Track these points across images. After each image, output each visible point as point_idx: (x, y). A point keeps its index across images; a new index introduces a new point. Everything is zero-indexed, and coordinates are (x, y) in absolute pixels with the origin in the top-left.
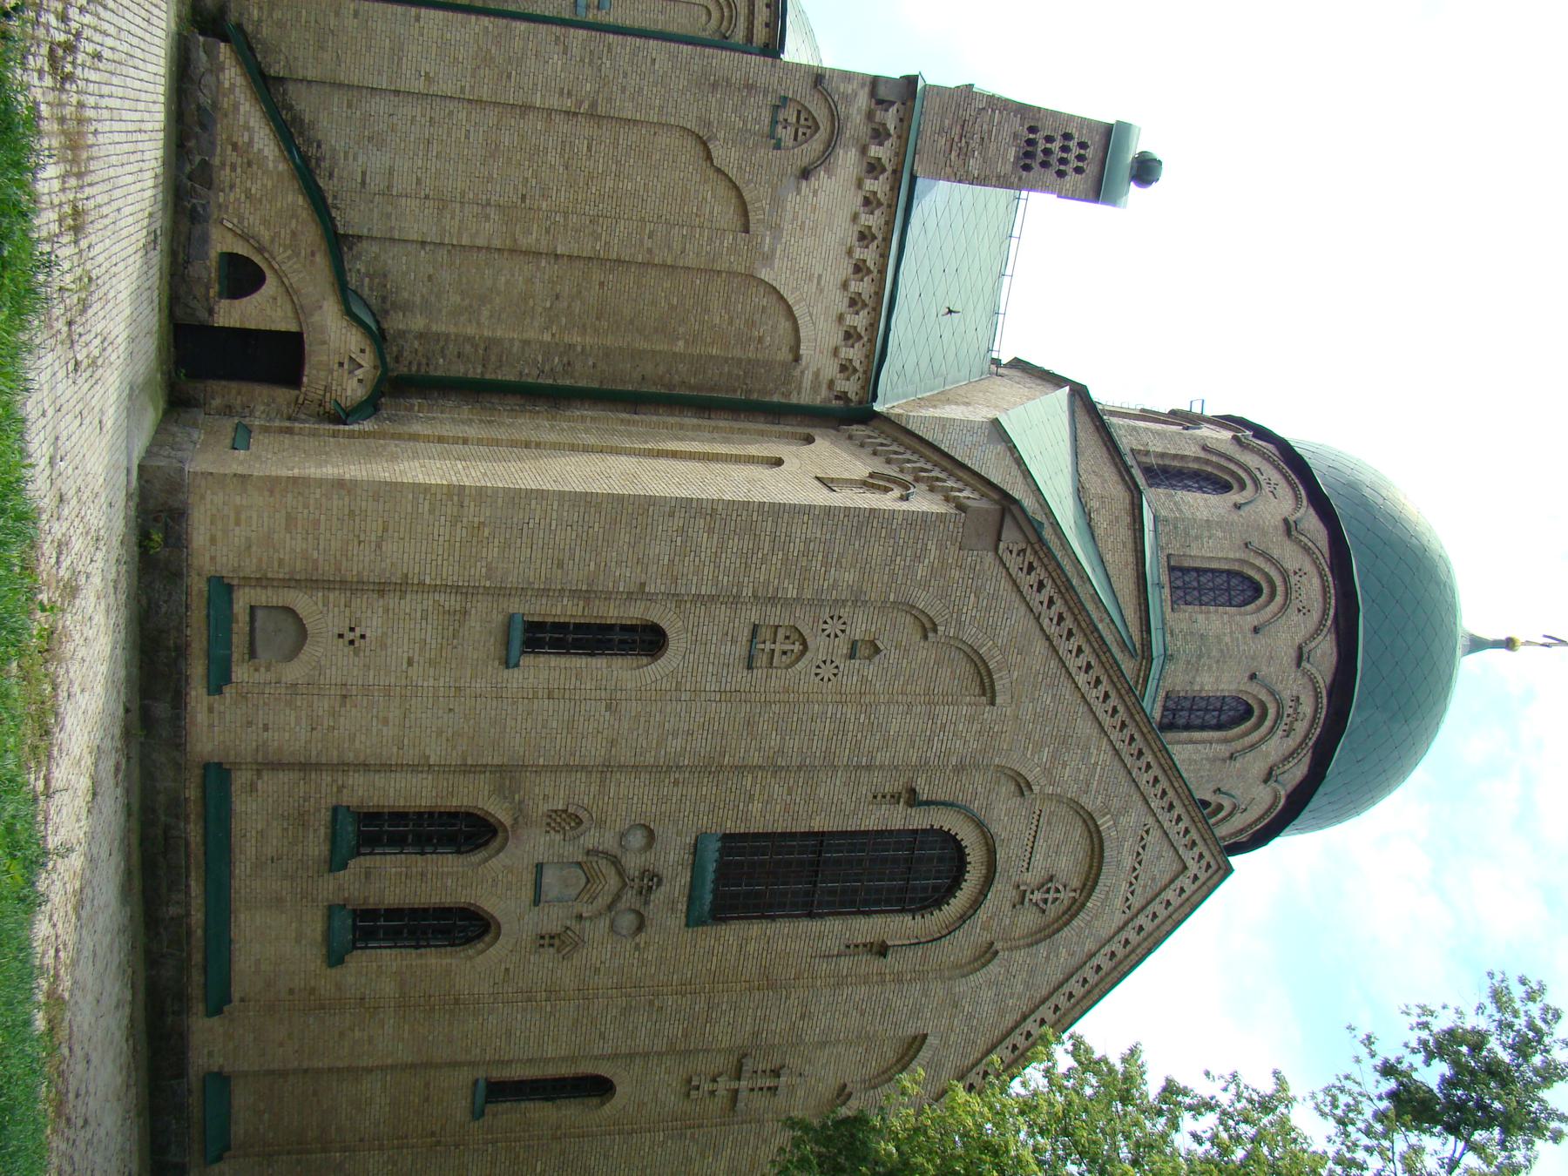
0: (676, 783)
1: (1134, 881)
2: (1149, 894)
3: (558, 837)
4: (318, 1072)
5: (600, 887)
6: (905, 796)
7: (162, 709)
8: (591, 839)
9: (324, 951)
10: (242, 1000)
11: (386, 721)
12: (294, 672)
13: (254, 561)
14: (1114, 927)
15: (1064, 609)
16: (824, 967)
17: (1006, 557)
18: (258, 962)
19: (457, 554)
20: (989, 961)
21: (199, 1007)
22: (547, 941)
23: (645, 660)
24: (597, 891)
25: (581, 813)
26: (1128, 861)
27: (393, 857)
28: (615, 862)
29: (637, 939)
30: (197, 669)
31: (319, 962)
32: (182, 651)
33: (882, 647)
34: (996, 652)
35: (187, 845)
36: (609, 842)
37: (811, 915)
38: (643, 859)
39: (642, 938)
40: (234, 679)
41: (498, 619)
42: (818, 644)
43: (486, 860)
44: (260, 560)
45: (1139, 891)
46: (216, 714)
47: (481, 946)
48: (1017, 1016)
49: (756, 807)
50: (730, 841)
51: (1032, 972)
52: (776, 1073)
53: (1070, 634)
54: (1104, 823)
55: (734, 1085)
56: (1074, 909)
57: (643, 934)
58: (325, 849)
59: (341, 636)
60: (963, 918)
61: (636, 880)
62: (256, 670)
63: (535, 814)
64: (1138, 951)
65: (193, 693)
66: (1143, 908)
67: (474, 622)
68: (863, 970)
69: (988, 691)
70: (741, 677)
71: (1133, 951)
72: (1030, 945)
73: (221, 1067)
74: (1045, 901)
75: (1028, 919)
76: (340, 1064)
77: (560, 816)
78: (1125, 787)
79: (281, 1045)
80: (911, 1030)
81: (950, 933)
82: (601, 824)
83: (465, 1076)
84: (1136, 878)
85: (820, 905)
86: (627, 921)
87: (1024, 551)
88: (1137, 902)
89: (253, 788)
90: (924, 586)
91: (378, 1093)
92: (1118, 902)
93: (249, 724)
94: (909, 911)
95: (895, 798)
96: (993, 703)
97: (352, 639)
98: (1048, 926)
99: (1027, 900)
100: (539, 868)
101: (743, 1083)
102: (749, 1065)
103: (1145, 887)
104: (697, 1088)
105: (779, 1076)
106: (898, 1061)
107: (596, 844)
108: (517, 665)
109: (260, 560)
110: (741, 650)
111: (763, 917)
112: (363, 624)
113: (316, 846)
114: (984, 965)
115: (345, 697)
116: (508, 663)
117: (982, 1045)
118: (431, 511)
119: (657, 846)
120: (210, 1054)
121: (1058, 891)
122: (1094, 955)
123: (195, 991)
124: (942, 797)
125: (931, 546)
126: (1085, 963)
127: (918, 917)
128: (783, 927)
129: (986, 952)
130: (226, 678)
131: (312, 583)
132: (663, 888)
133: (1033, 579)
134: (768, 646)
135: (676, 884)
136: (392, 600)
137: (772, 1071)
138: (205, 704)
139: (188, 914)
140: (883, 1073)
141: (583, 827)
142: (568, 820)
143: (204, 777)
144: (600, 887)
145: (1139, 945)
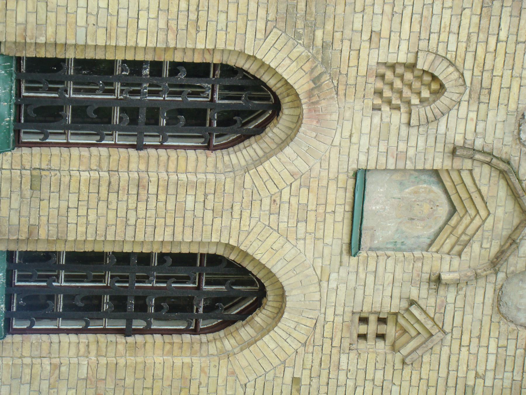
43: (259, 161)
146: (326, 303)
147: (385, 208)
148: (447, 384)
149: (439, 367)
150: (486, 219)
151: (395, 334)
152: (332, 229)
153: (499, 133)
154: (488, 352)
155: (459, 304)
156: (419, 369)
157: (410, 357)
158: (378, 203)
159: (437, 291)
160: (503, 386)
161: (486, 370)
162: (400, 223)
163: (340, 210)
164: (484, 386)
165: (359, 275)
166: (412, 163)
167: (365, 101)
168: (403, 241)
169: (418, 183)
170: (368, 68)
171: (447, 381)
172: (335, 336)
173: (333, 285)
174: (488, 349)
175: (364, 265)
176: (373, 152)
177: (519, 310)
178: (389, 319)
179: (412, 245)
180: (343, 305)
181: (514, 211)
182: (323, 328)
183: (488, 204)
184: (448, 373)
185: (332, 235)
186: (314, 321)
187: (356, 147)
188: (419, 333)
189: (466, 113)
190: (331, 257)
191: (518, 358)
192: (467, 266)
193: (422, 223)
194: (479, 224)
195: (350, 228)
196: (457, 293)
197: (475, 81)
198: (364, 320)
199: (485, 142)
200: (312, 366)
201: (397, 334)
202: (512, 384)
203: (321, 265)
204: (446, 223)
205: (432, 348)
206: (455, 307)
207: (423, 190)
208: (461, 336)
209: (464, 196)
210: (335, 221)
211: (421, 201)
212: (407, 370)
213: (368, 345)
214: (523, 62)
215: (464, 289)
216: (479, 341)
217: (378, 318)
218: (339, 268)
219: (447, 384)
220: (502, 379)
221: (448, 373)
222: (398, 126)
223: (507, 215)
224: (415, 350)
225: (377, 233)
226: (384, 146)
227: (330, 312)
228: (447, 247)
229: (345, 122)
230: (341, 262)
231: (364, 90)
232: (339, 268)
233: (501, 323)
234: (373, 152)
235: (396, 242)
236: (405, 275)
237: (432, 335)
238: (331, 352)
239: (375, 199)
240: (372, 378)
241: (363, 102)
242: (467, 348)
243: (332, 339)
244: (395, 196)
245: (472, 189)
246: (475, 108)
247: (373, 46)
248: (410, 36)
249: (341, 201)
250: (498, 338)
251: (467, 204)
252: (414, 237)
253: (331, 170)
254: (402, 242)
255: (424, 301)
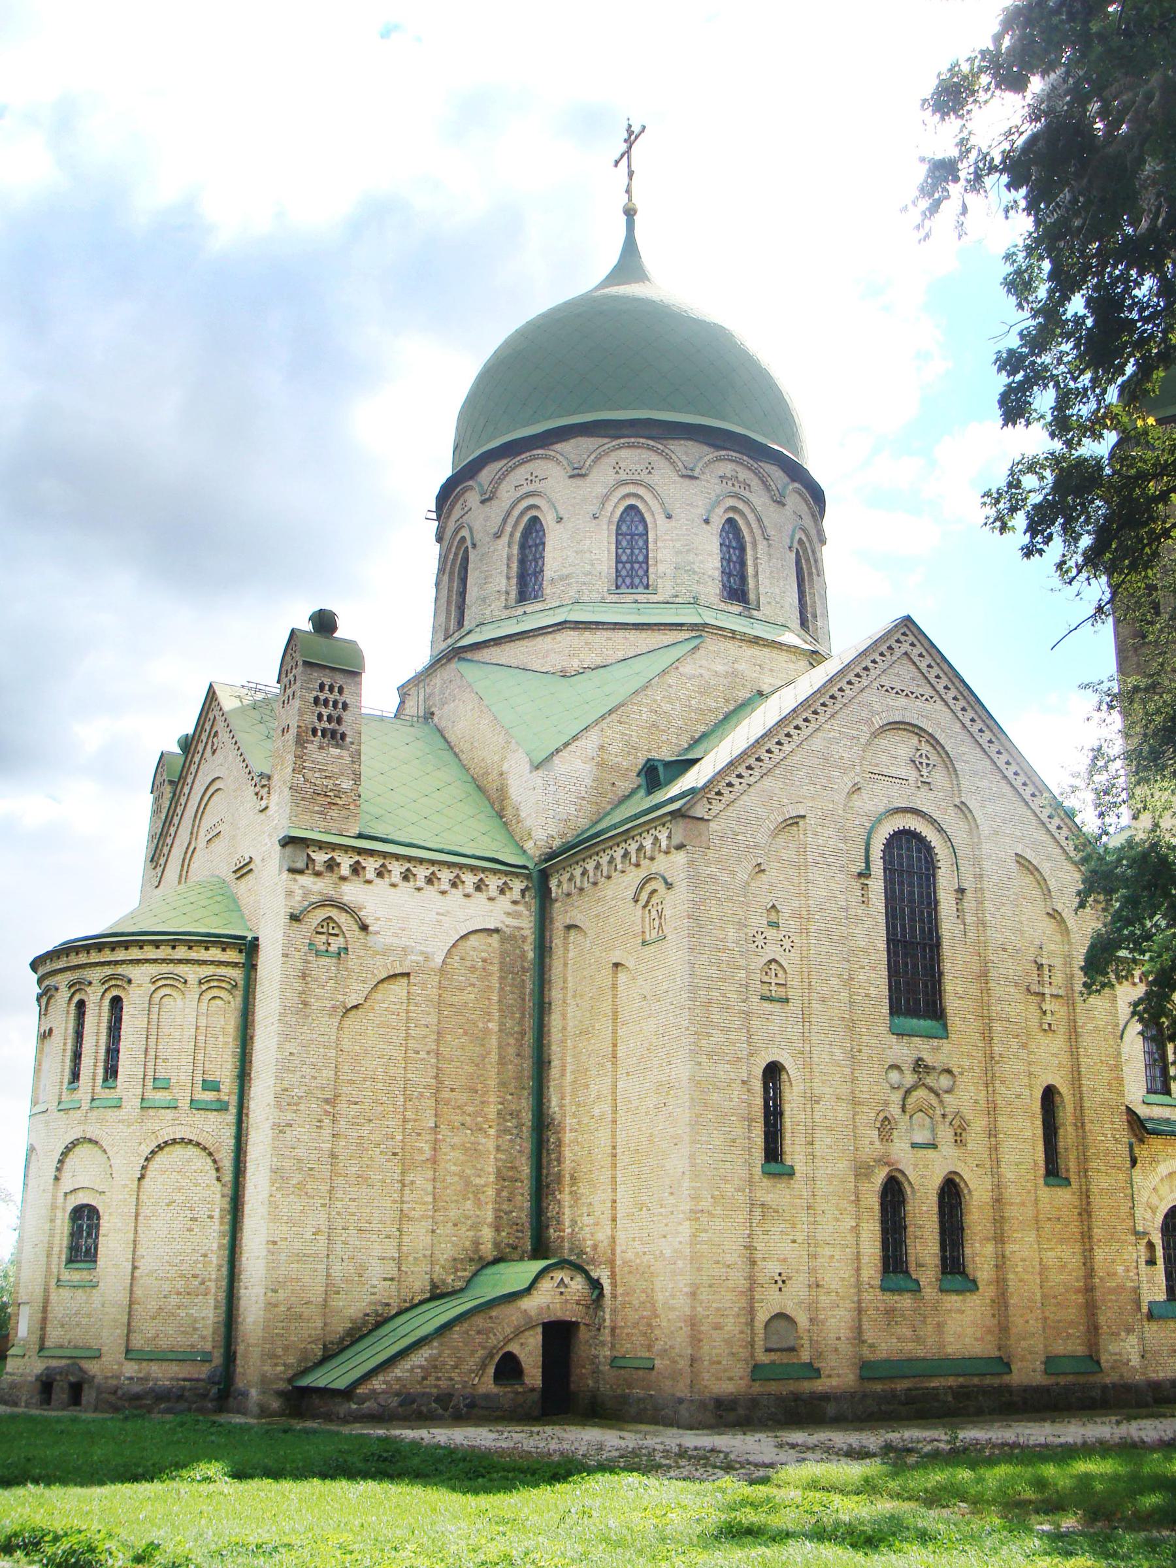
0: (860, 1051)
1: (914, 695)
2: (923, 682)
3: (895, 1133)
4: (1044, 1296)
6: (863, 880)
7: (831, 1409)
8: (895, 1110)
9: (968, 1294)
10: (999, 1349)
11: (832, 1257)
12: (802, 1319)
13: (741, 1350)
14: (945, 709)
15: (744, 766)
16: (972, 935)
17: (713, 813)
18: (977, 1339)
19: (731, 1213)
20: (968, 808)
21: (1006, 1379)
22: (958, 1138)
23: (784, 1077)
25: (881, 1117)
26: (902, 701)
27: (908, 1248)
28: (908, 1092)
29: (956, 1073)
30: (807, 1386)
31: (975, 1297)
32: (796, 1397)
33: (771, 904)
34: (772, 817)
35: (909, 1389)
36: (896, 1097)
37: (938, 945)
39: (955, 1070)
40: (808, 1361)
41: (766, 1182)
42: (772, 951)
43: (910, 1183)
44: (740, 1346)
45: (921, 691)
46: (832, 1372)
47: (962, 1185)
48: (1003, 783)
49: (873, 991)
50: (895, 1010)
51: (975, 774)
52: (1040, 967)
53: (759, 759)
54: (878, 722)
55: (1048, 998)
56: (934, 742)
58: (907, 1296)
59: (780, 1289)
60: (940, 830)
62: (803, 1346)
64: (961, 689)
65: (820, 1388)
66: (933, 686)
67: (768, 1198)
68: (973, 905)
69: (795, 820)
70: (794, 1007)
71: (961, 693)
72: (957, 776)
73: (1041, 1363)
74: (928, 765)
75: (939, 777)
76: (1038, 1281)
78: (854, 706)
79: (1027, 1322)
80: (1014, 866)
81: (950, 840)
82: (886, 1104)
83: (1045, 1193)
84: (912, 693)
85: (931, 939)
86: (944, 1081)
87: (708, 798)
88: (929, 692)
89: (872, 1346)
90: (733, 873)
91: (1054, 1253)
92: (928, 706)
93: (836, 1350)
94: (934, 870)
95: (865, 887)
96: (804, 817)
97: (782, 1282)
98: (943, 761)
99: (927, 781)
100: (914, 1146)
101: (1047, 991)
102: (1035, 988)
103: (918, 686)
104: (1050, 1025)
105: (1042, 965)
106: (1032, 874)
108: (792, 1167)
109: (740, 1346)
110: (776, 1007)
111: (940, 982)
112: (773, 1274)
113: (905, 1302)
114: (970, 811)
115: (818, 1286)
116: (791, 1173)
117: (1023, 809)
118: (706, 1231)
119: (899, 1062)
120: (1034, 1371)
121: (921, 756)
122: (963, 724)
123: (996, 1381)
124: (862, 853)
125: (709, 870)
126: (969, 731)
127: (939, 864)
128: (947, 967)
129: (961, 810)
130: (810, 1365)
131: (751, 1311)
132: (925, 1057)
133: (725, 791)
134: (773, 988)
135: (922, 1048)
136: (758, 1255)
137: (1038, 969)
138: (825, 1380)
139: (950, 1387)
140: (1039, 884)
141: (889, 1116)
143: (869, 1379)
145: (957, 688)
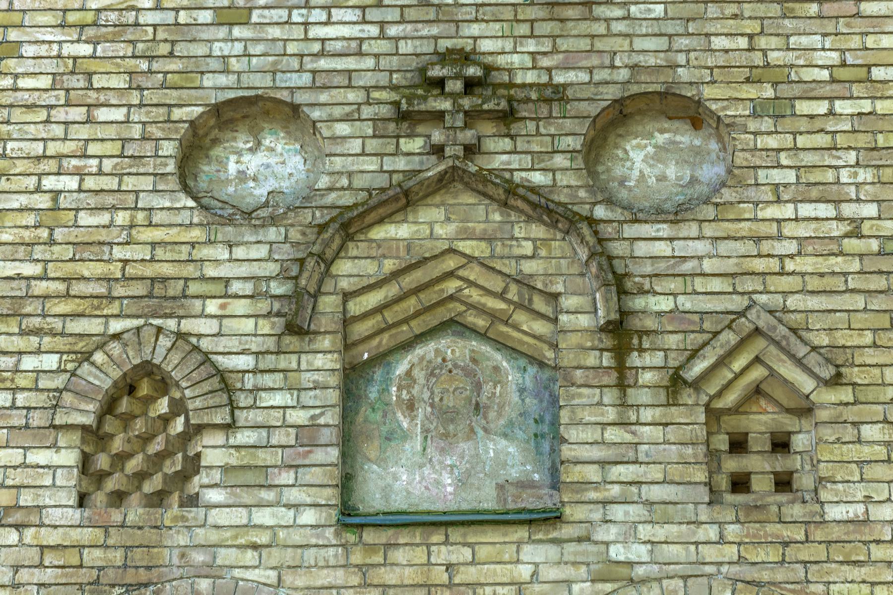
5: (473, 273)
24: (497, 284)
38: (343, 129)
57: (708, 92)
61: (438, 136)
63: (92, 557)
77: (121, 458)
107: (263, 306)
142: (139, 426)
144: (473, 273)
146: (690, 563)
147: (452, 467)
148: (881, 292)
149: (839, 311)
150: (464, 255)
151: (769, 413)
152: (492, 566)
153: (262, 251)
154: (792, 220)
155: (673, 285)
156: (848, 350)
157: (817, 370)
158: (437, 482)
159: (644, 333)
160: (873, 183)
161: (839, 218)
162: (486, 430)
163: (442, 555)
164: (879, 218)
165: (610, 499)
166: (322, 414)
167: (167, 523)
168: (532, 421)
169: (387, 405)
170: (87, 524)
171: (876, 291)
172: (778, 537)
173: (640, 552)
174: (785, 220)
175: (586, 490)
176: (294, 495)
177: (694, 181)
178: (730, 430)
179: (541, 401)
180: (692, 526)
181: (443, 205)
182: (758, 566)
183: (427, 255)
184: (853, 291)
185: (509, 566)
186: (740, 585)
187: (282, 534)
188: (757, 360)
189: (208, 320)
190: (566, 563)
191: (802, 160)
192: (579, 280)
193: (487, 388)
194: (477, 268)
195: (488, 528)
196: (648, 292)
197: (133, 310)
198: (740, 484)
199: (278, 275)
200: (864, 582)
201: (770, 409)
202: (868, 166)
203: (589, 584)
204: (483, 336)
205: (794, 331)
206: (685, 293)
207: (404, 392)
208: (758, 274)
209: (411, 304)
210: (473, 563)
211: (432, 393)
212: (854, 374)
213: (803, 467)
214: (97, 227)
215: (637, 279)
216: (767, 238)
217: (731, 452)
218: (596, 543)
219: (881, 292)
220: (858, 185)
221: (853, 291)
222: (232, 451)
223: (453, 217)
224: (799, 362)
225: (514, 473)
226: (280, 474)
227: (710, 553)
228: (540, 327)
229: (219, 562)
230: (579, 540)
231: (140, 528)
232: (596, 543)
233: (718, 200)
234: (294, 495)
235: (536, 435)
236: (606, 400)
237: (757, 331)
238: (820, 543)
239: (427, 488)
240: (883, 447)
241: (170, 528)
242: (787, 261)
243: (786, 544)
244: (419, 448)
245: (392, 290)
246: (198, 303)
247: (34, 519)
248: (18, 448)
249: (420, 555)
250: (756, 204)
251: (429, 297)
252: (523, 400)
253: (340, 582)
254: (536, 421)
255: (672, 355)
